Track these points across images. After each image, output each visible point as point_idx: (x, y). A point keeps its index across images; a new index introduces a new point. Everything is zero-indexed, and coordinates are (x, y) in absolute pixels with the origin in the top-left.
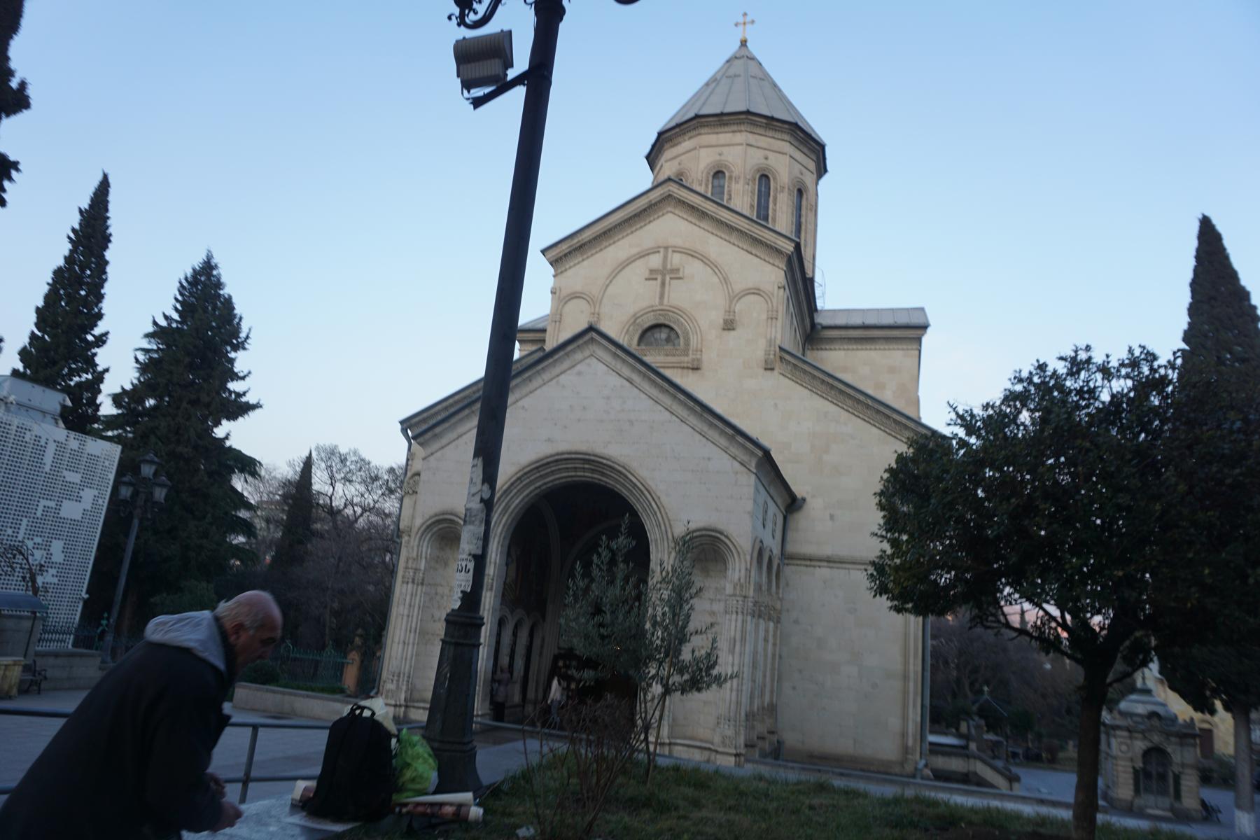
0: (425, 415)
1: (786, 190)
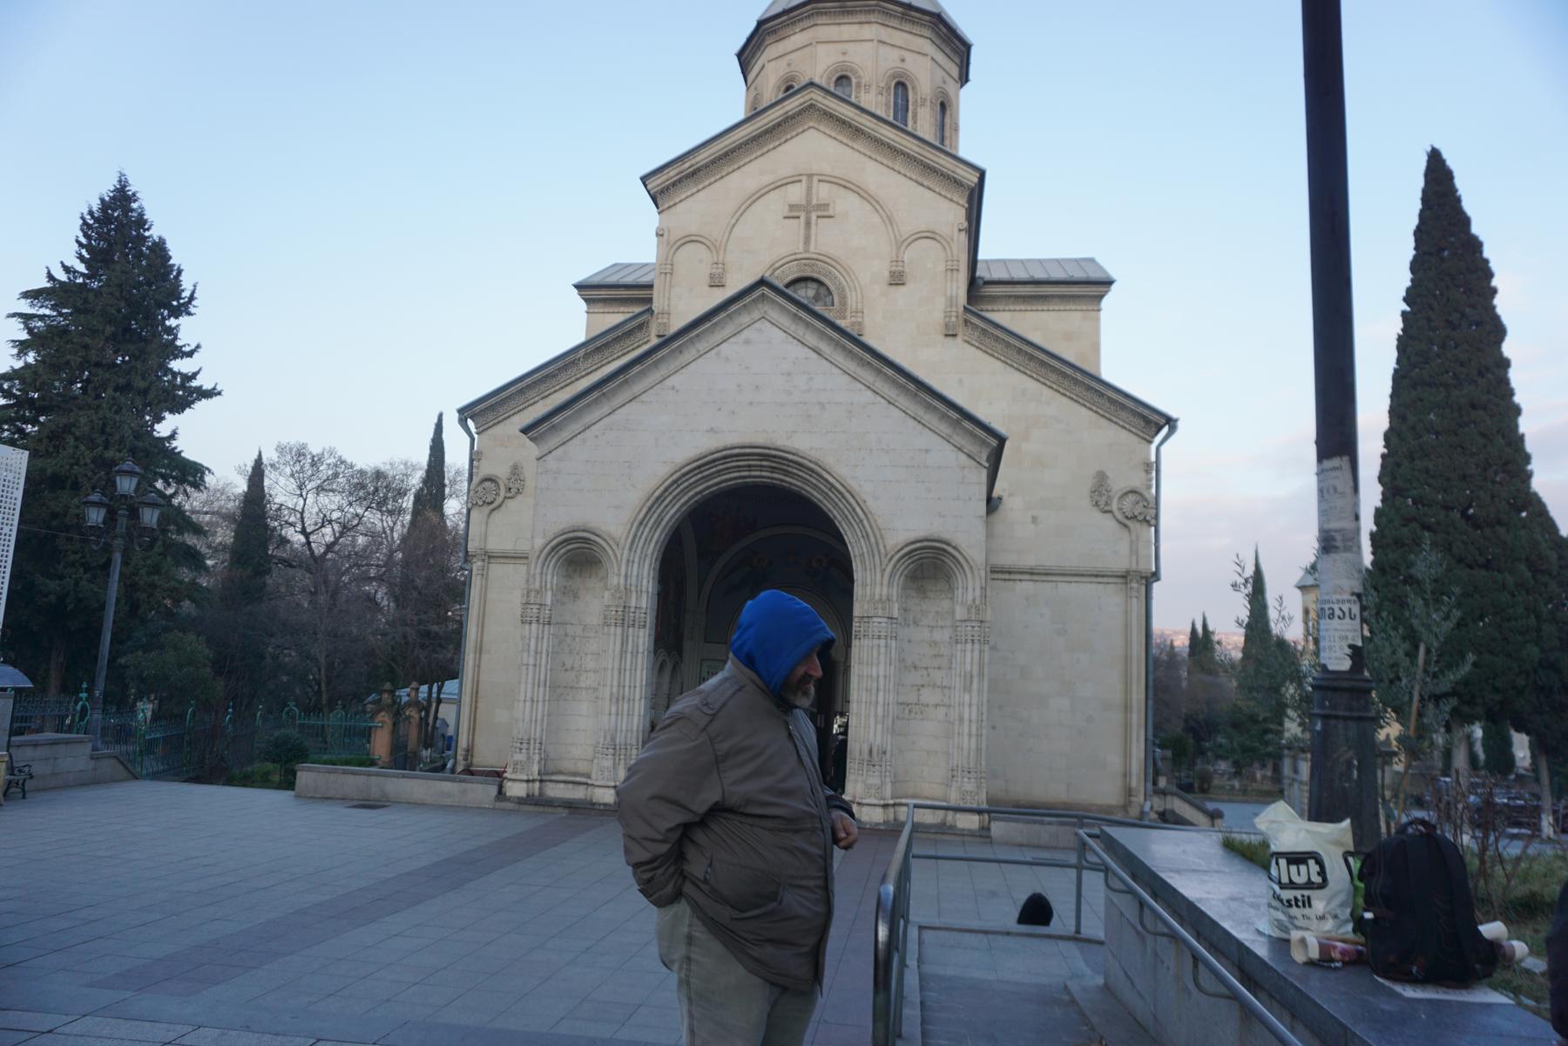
0: (493, 401)
1: (928, 103)
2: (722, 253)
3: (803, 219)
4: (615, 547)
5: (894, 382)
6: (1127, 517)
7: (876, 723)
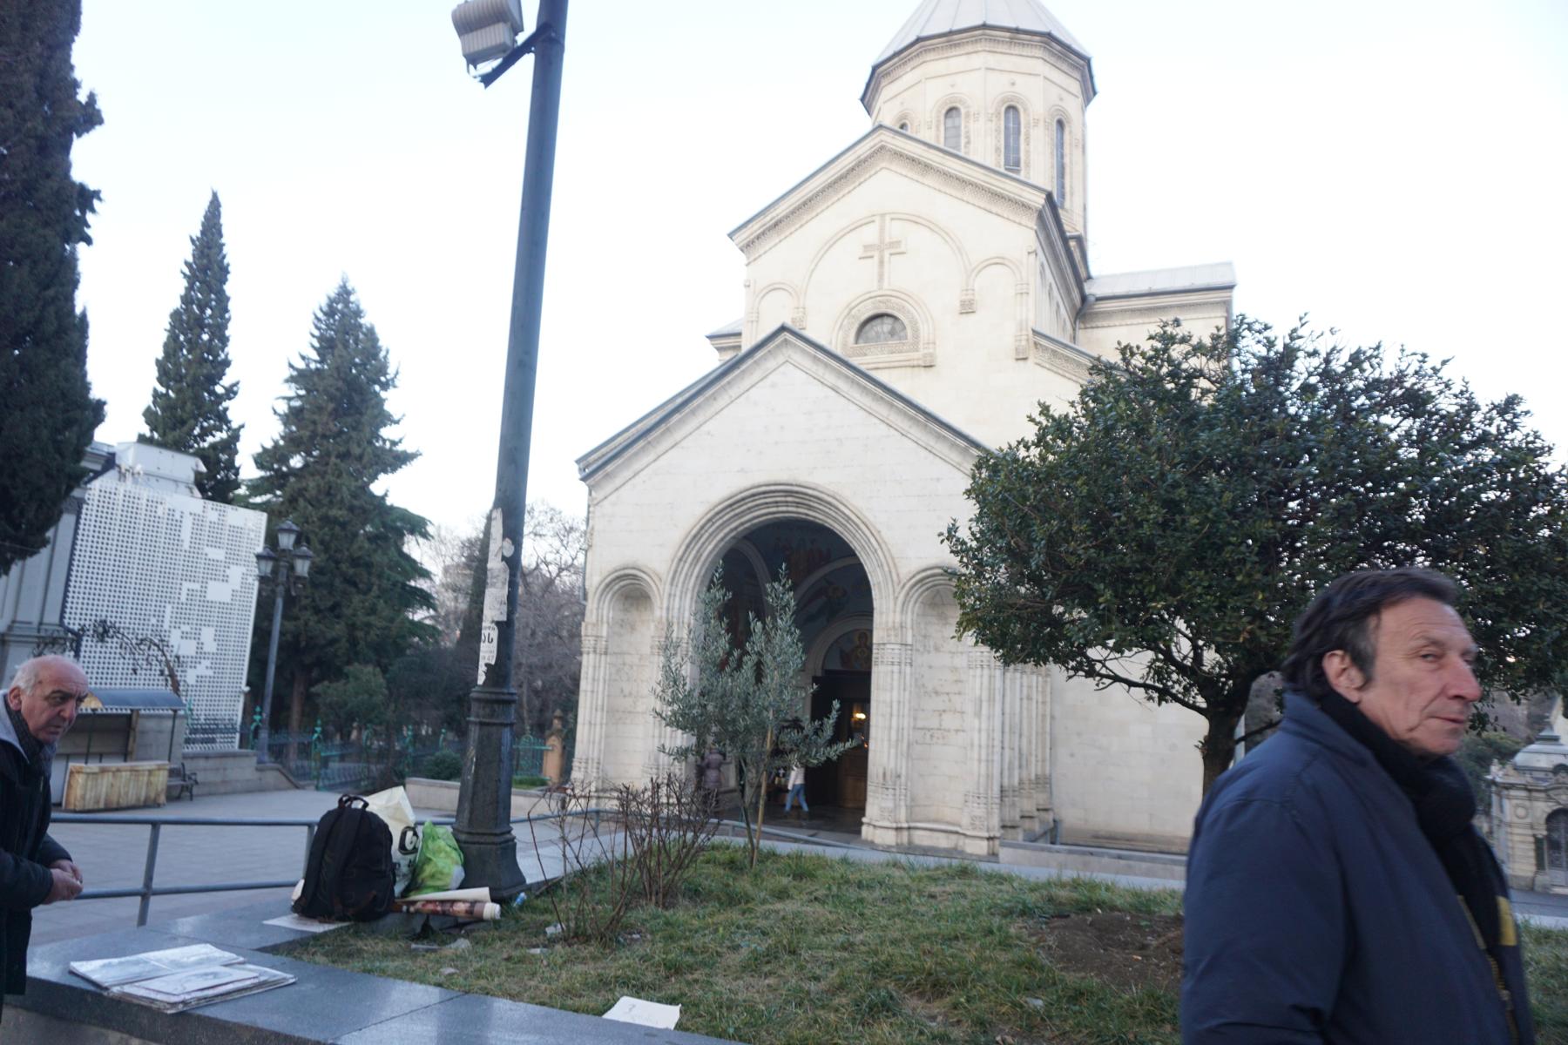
1: (1042, 123)
3: (876, 259)
5: (905, 414)
7: (889, 748)
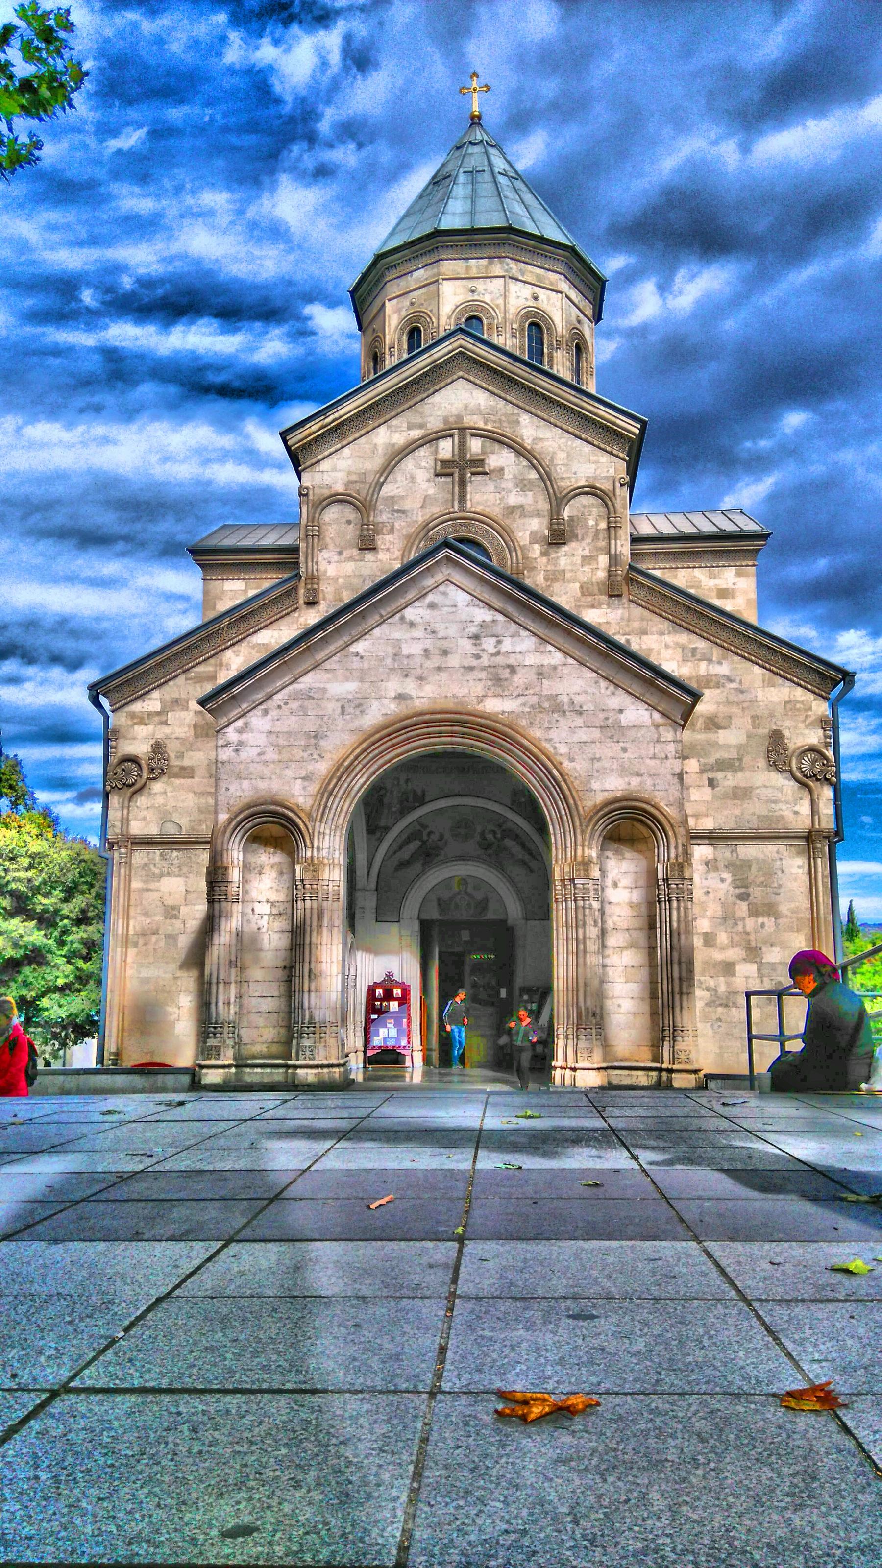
2: (372, 514)
3: (456, 475)
4: (306, 820)
6: (806, 776)
